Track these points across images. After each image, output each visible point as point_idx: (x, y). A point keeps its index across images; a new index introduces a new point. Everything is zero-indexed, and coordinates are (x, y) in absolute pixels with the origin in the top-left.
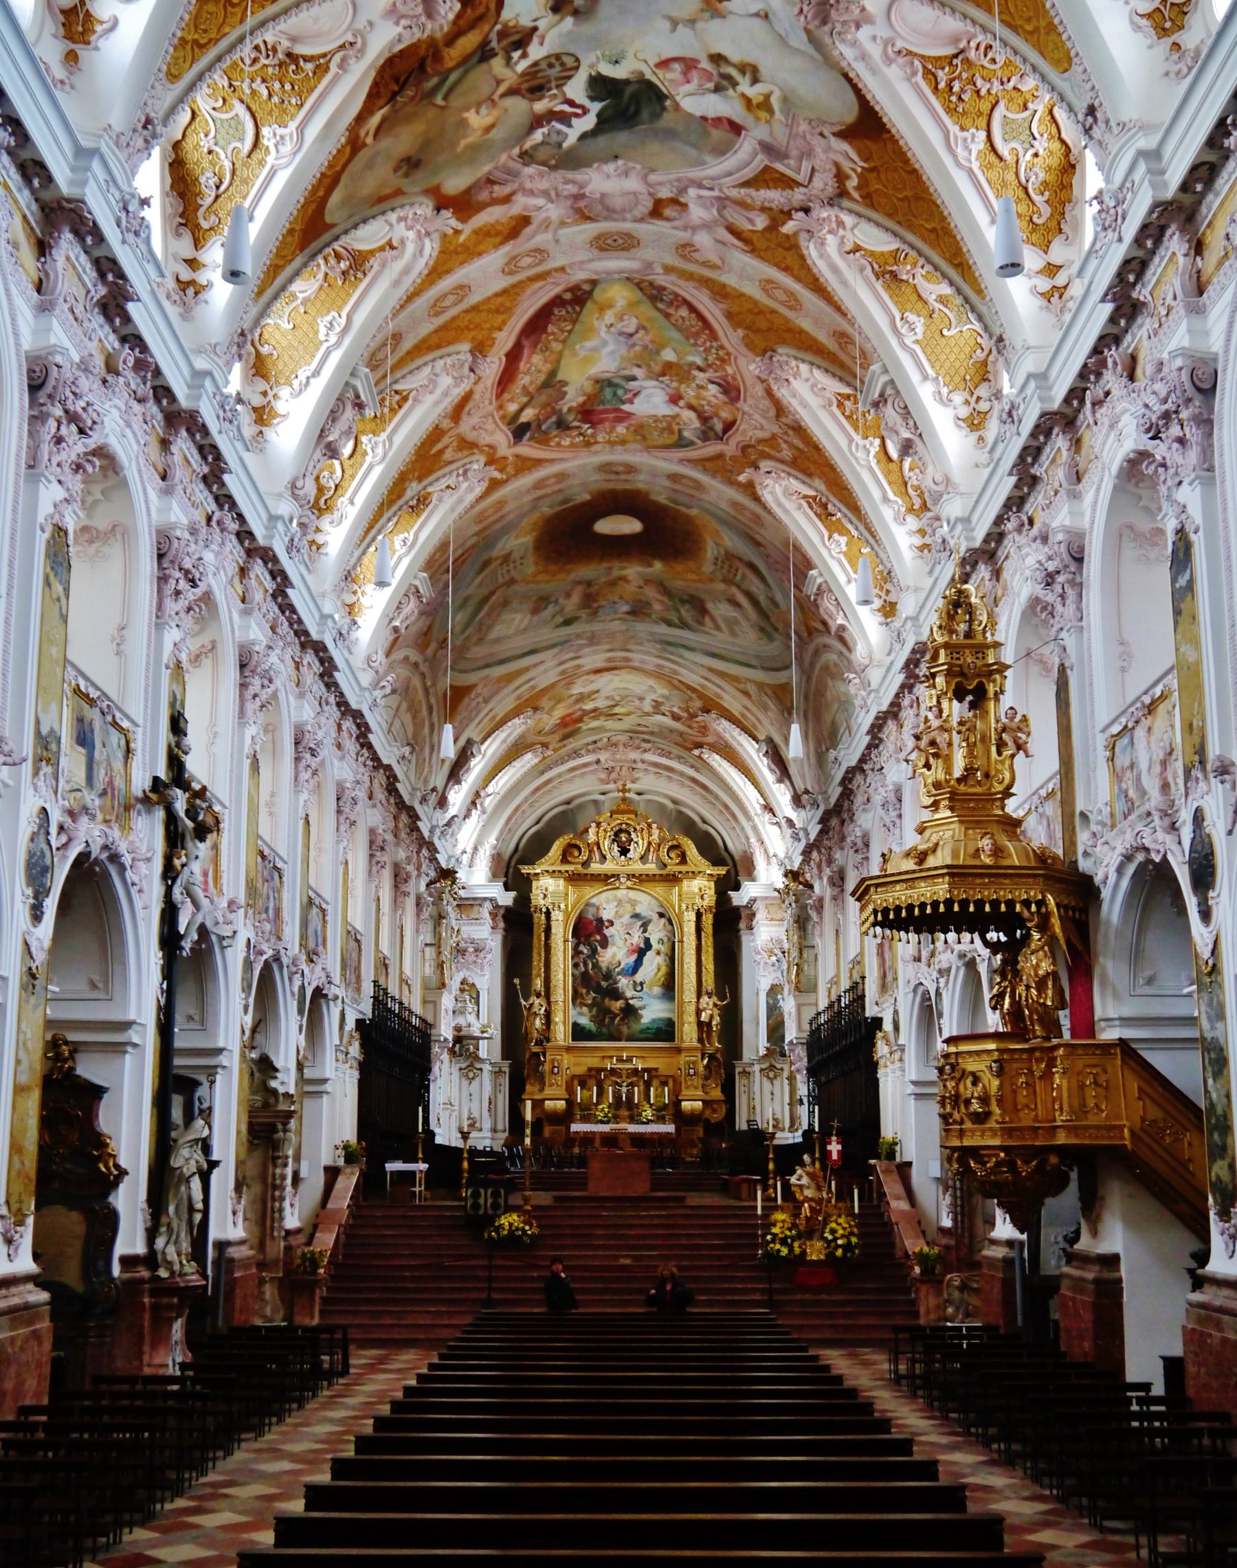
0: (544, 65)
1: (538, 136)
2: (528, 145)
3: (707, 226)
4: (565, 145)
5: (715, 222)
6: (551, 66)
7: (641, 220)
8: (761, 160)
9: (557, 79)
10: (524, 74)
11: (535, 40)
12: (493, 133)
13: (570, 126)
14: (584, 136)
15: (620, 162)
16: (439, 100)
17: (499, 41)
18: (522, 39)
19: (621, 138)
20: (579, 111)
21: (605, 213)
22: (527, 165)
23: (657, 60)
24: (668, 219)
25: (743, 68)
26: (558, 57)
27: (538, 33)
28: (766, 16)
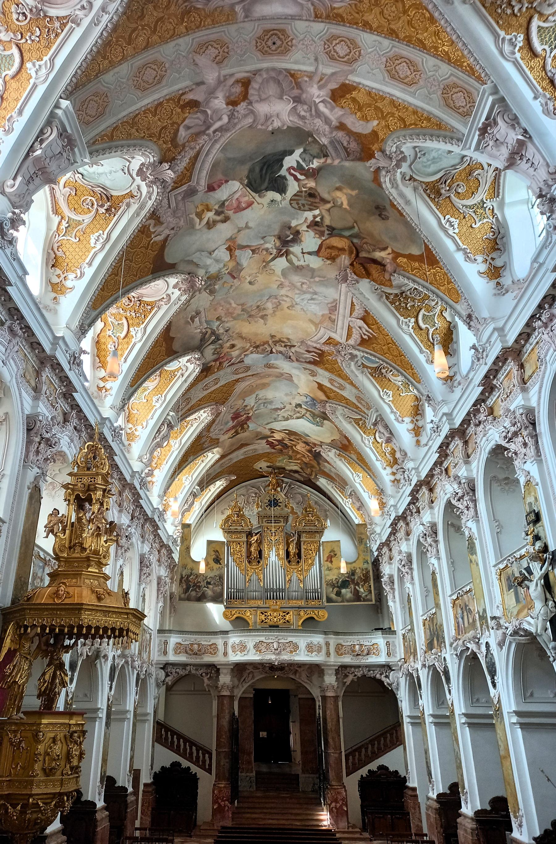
0: (307, 207)
1: (315, 164)
2: (322, 160)
3: (211, 93)
4: (301, 150)
5: (207, 101)
6: (303, 205)
7: (256, 72)
8: (193, 183)
9: (301, 196)
10: (317, 208)
11: (309, 222)
12: (337, 185)
13: (298, 162)
14: (291, 153)
15: (270, 128)
16: (356, 229)
17: (324, 231)
18: (314, 225)
19: (269, 150)
20: (292, 171)
21: (281, 78)
22: (324, 145)
23: (253, 206)
24: (237, 81)
25: (215, 222)
26: (300, 209)
27: (306, 224)
28: (210, 254)
